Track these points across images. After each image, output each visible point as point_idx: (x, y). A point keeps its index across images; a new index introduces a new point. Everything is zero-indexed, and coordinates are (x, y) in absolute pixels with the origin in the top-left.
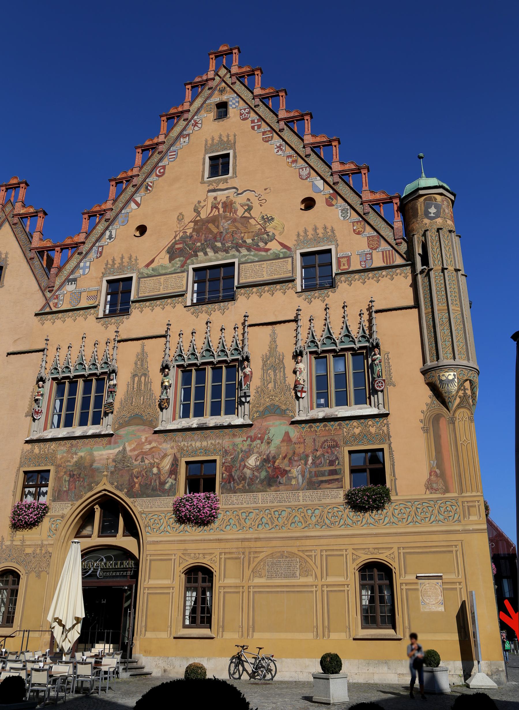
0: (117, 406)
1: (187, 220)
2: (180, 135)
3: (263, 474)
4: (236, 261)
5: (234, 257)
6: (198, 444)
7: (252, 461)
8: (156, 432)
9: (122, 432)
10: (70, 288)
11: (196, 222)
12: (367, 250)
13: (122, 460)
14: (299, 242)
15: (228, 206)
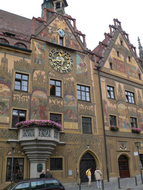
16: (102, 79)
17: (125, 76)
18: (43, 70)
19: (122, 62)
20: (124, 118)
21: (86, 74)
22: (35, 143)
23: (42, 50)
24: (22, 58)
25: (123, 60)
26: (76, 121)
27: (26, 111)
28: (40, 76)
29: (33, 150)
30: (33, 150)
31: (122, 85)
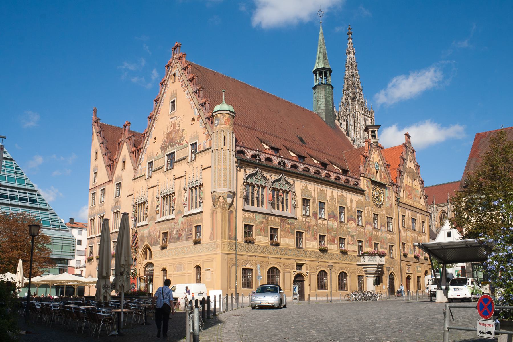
0: (148, 214)
1: (165, 133)
2: (164, 92)
3: (177, 236)
4: (175, 150)
5: (175, 149)
6: (164, 226)
7: (175, 232)
8: (156, 223)
9: (149, 223)
10: (140, 167)
11: (167, 134)
12: (206, 141)
13: (149, 233)
14: (190, 141)
15: (174, 125)
16: (400, 209)
17: (410, 202)
18: (369, 206)
19: (410, 187)
20: (409, 244)
21: (391, 206)
22: (376, 266)
23: (368, 187)
24: (359, 197)
25: (411, 185)
26: (386, 248)
27: (362, 241)
28: (368, 212)
29: (373, 270)
30: (373, 270)
31: (410, 212)
